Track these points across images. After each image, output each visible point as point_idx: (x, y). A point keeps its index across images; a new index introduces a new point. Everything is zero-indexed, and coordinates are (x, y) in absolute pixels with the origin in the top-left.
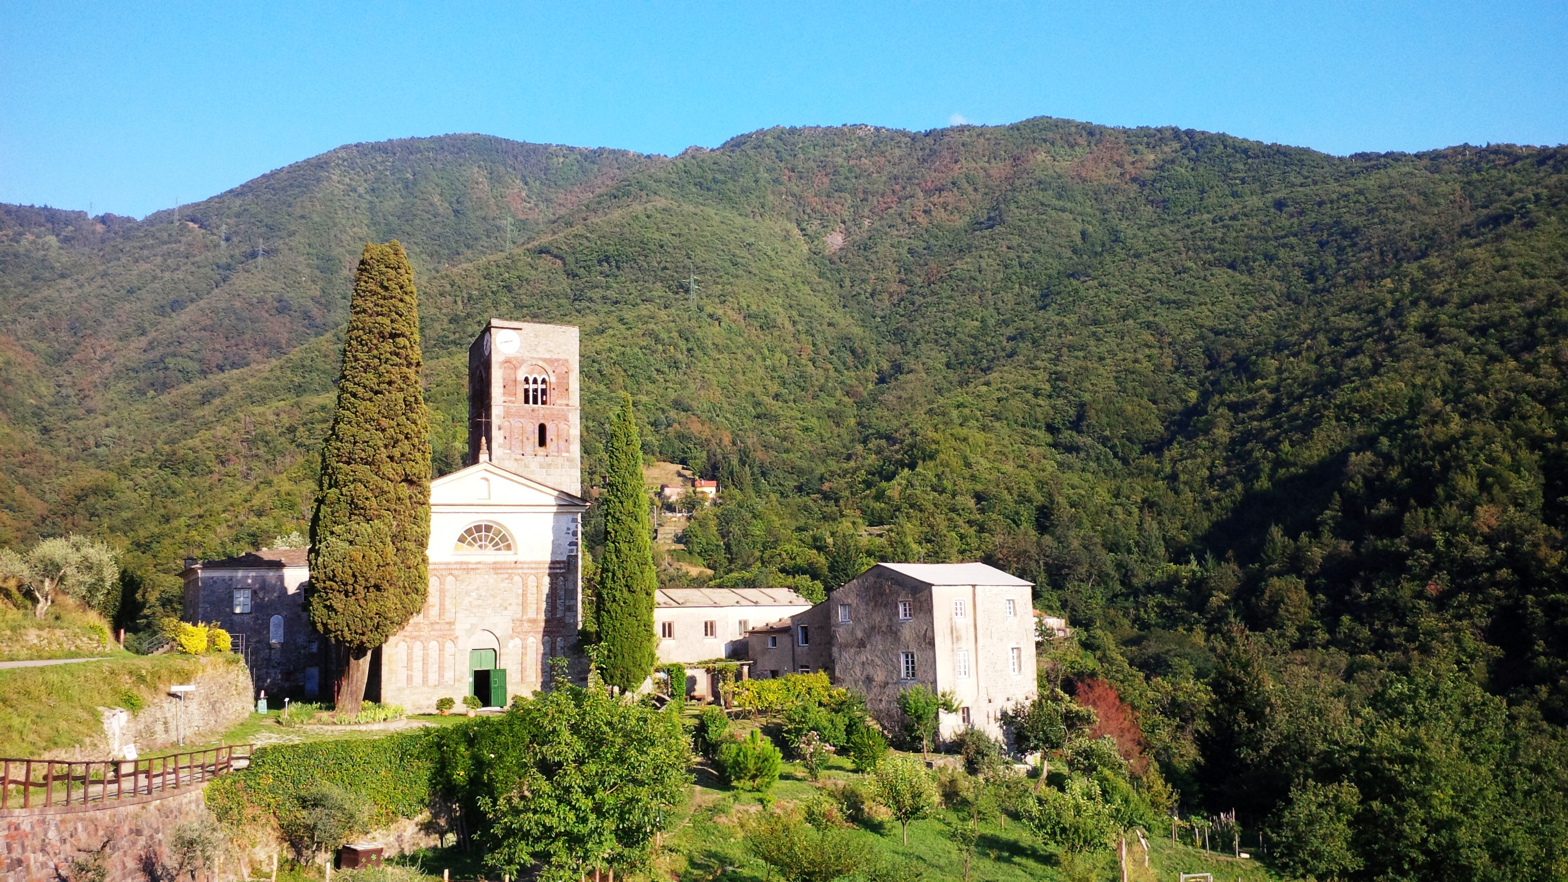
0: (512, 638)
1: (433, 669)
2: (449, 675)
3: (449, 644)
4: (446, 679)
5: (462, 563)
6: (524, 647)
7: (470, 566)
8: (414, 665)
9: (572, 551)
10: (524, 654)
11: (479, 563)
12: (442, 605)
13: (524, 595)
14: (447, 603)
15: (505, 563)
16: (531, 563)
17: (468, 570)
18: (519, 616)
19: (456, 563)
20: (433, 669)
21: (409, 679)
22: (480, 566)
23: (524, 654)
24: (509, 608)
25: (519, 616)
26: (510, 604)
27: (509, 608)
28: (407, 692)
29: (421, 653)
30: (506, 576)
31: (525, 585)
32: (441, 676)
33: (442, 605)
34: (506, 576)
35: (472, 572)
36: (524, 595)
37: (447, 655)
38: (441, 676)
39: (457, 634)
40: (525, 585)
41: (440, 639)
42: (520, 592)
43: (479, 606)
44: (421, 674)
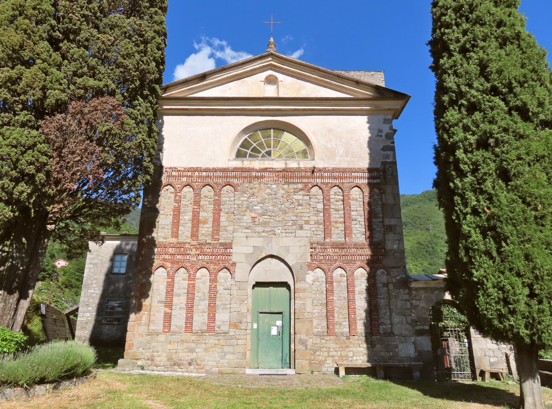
0: (311, 267)
1: (202, 305)
2: (222, 317)
3: (223, 275)
4: (217, 323)
5: (242, 170)
6: (329, 282)
7: (254, 174)
8: (175, 300)
9: (387, 156)
10: (329, 292)
11: (265, 170)
12: (216, 221)
13: (326, 211)
14: (222, 219)
15: (298, 170)
16: (334, 170)
17: (251, 179)
18: (320, 237)
19: (235, 170)
20: (202, 305)
21: (168, 318)
22: (266, 174)
23: (329, 292)
24: (306, 227)
25: (320, 237)
26: (307, 222)
27: (306, 227)
28: (162, 338)
29: (185, 284)
30: (300, 186)
31: (326, 200)
32: (212, 318)
33: (216, 221)
34: (300, 186)
35: (256, 182)
36: (326, 211)
37: (220, 288)
38: (212, 318)
39: (234, 259)
40: (326, 200)
41: (212, 267)
42: (320, 206)
43: (265, 224)
44: (184, 313)
